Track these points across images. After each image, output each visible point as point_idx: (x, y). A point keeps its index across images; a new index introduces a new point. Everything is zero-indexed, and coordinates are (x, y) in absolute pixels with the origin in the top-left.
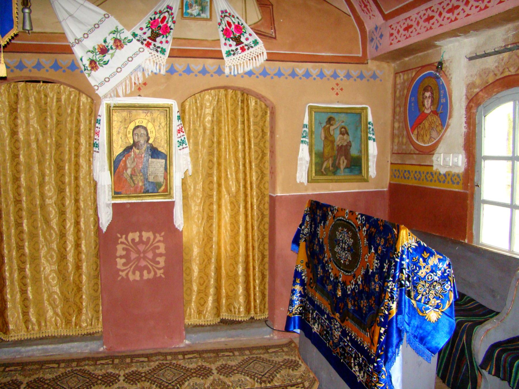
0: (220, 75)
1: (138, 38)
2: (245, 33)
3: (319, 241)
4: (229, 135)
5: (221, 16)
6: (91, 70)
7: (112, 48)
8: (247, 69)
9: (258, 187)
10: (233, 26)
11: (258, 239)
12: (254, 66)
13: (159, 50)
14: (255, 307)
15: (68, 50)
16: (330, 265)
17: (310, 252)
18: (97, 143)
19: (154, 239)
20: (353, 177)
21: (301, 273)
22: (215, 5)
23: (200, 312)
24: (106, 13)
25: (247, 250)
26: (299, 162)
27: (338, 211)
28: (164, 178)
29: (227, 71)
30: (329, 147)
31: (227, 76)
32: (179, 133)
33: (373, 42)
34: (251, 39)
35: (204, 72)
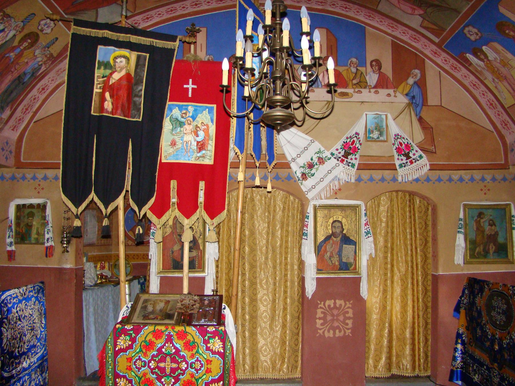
0: (394, 182)
1: (335, 156)
2: (413, 150)
3: (477, 308)
4: (399, 227)
5: (395, 138)
6: (302, 180)
7: (316, 164)
8: (415, 177)
9: (423, 267)
10: (404, 145)
11: (423, 309)
12: (420, 174)
13: (350, 164)
14: (419, 365)
15: (287, 166)
16: (487, 326)
17: (469, 318)
18: (306, 232)
19: (345, 306)
20: (500, 260)
21: (462, 334)
22: (390, 129)
23: (375, 367)
24: (312, 139)
25: (414, 318)
26: (456, 248)
27: (493, 284)
28: (354, 260)
29: (400, 179)
30: (480, 236)
31: (400, 183)
32: (366, 226)
33: (514, 152)
34: (417, 155)
35: (383, 180)
